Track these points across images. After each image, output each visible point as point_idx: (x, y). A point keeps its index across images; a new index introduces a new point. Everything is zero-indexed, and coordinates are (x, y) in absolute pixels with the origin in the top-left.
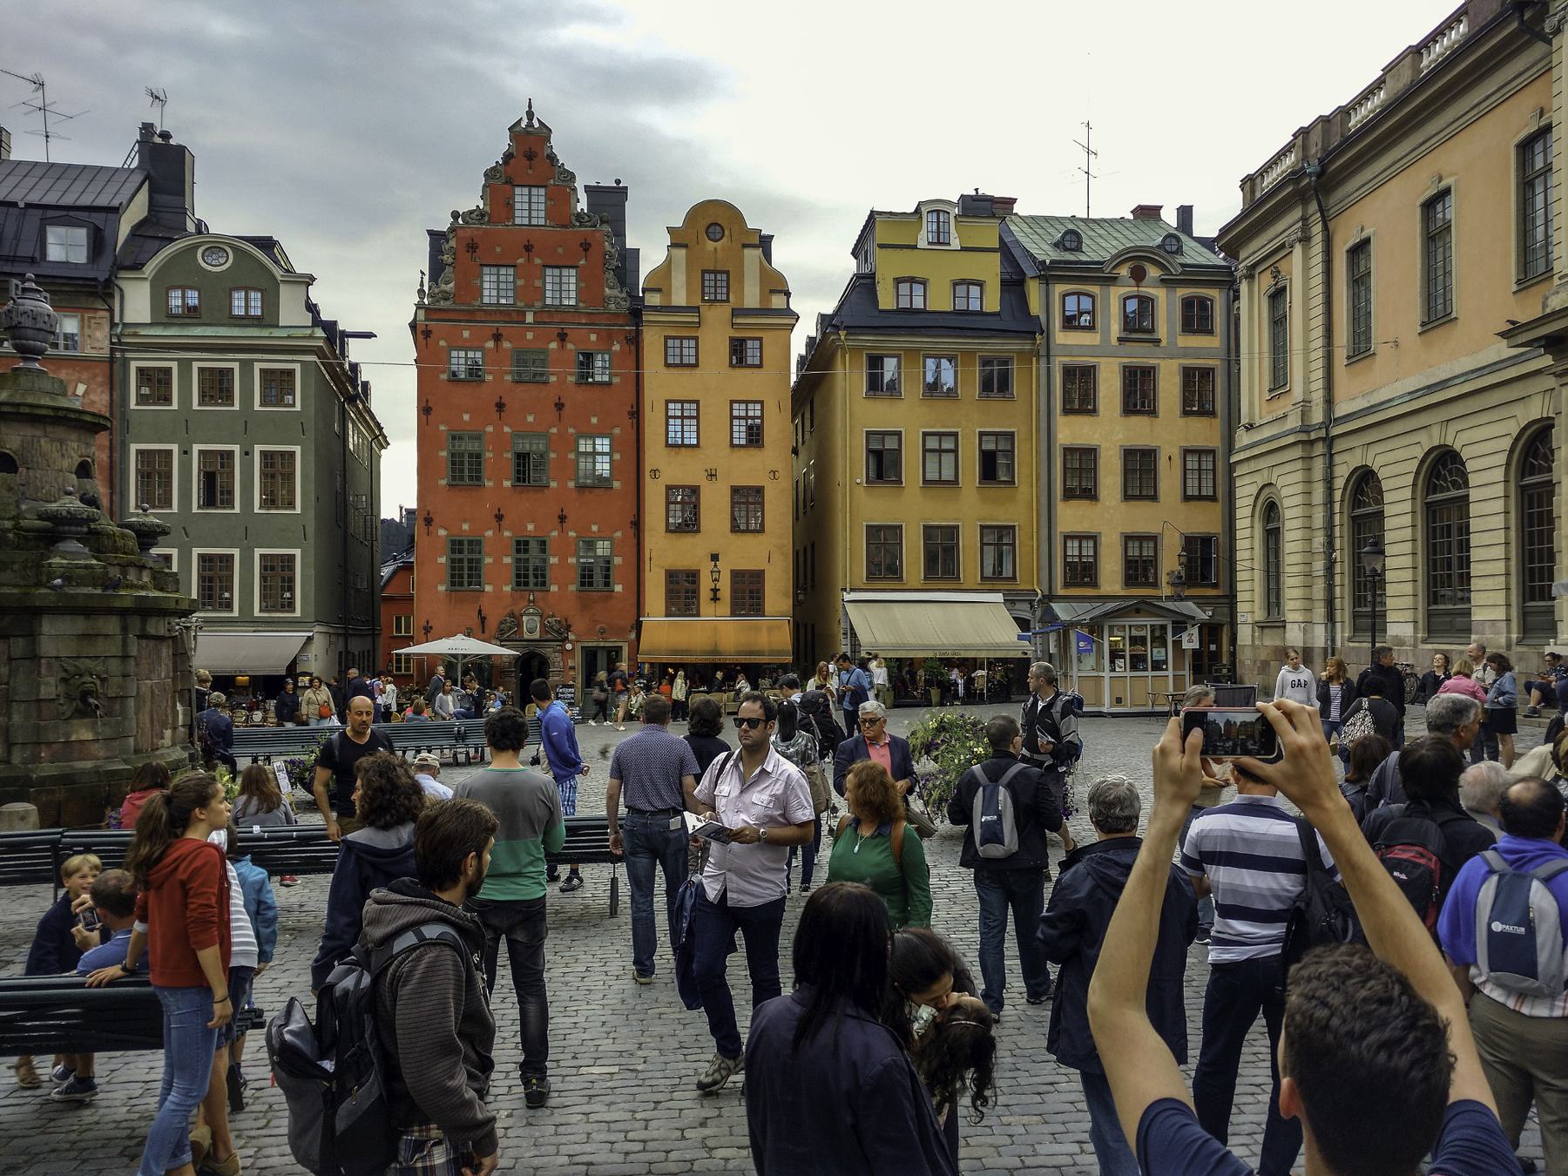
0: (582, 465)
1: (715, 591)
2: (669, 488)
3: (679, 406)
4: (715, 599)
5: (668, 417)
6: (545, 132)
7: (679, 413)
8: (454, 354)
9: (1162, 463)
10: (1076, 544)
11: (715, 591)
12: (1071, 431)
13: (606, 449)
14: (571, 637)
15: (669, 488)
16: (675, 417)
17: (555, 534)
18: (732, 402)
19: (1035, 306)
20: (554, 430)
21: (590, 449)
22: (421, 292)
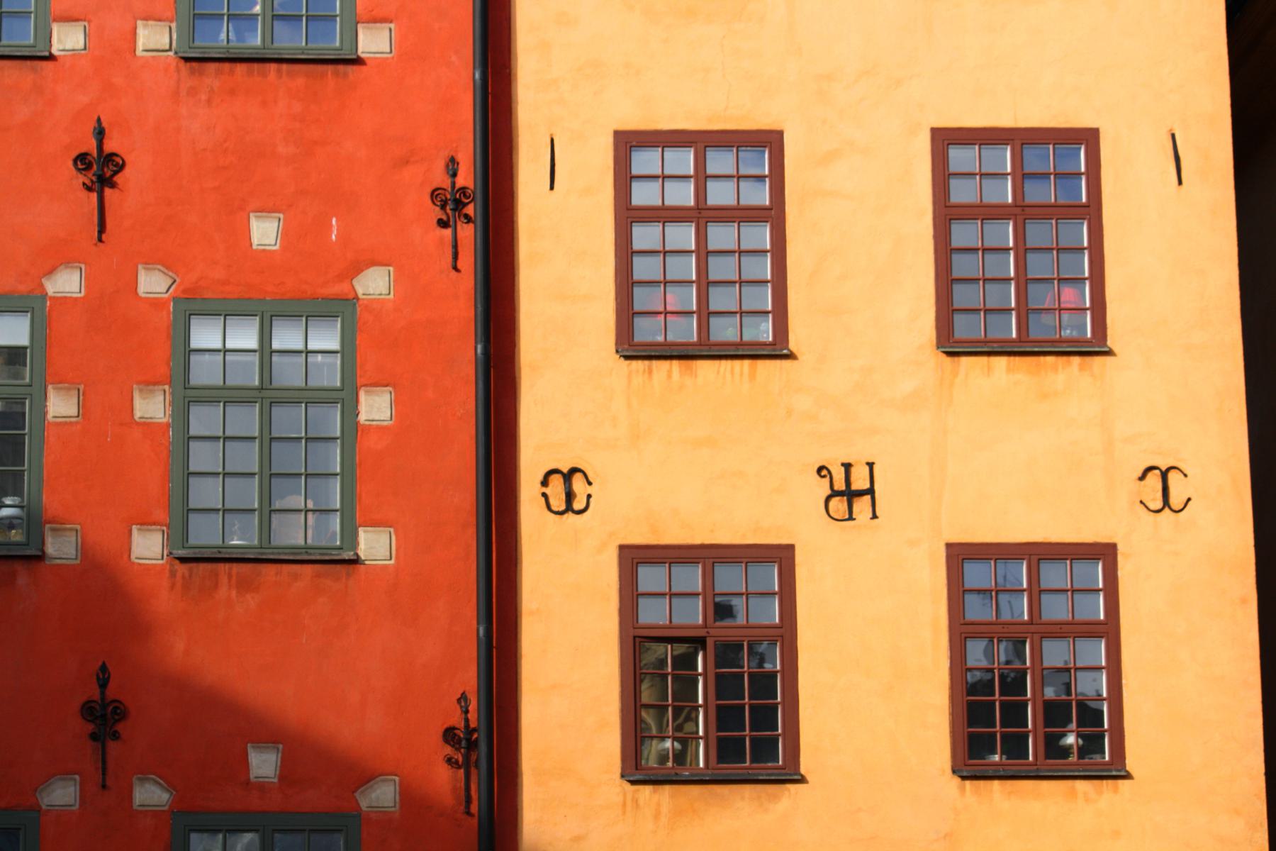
0: (203, 457)
2: (634, 558)
3: (683, 161)
5: (628, 216)
7: (683, 195)
15: (634, 558)
16: (664, 215)
17: (62, 795)
18: (944, 140)
20: (66, 283)
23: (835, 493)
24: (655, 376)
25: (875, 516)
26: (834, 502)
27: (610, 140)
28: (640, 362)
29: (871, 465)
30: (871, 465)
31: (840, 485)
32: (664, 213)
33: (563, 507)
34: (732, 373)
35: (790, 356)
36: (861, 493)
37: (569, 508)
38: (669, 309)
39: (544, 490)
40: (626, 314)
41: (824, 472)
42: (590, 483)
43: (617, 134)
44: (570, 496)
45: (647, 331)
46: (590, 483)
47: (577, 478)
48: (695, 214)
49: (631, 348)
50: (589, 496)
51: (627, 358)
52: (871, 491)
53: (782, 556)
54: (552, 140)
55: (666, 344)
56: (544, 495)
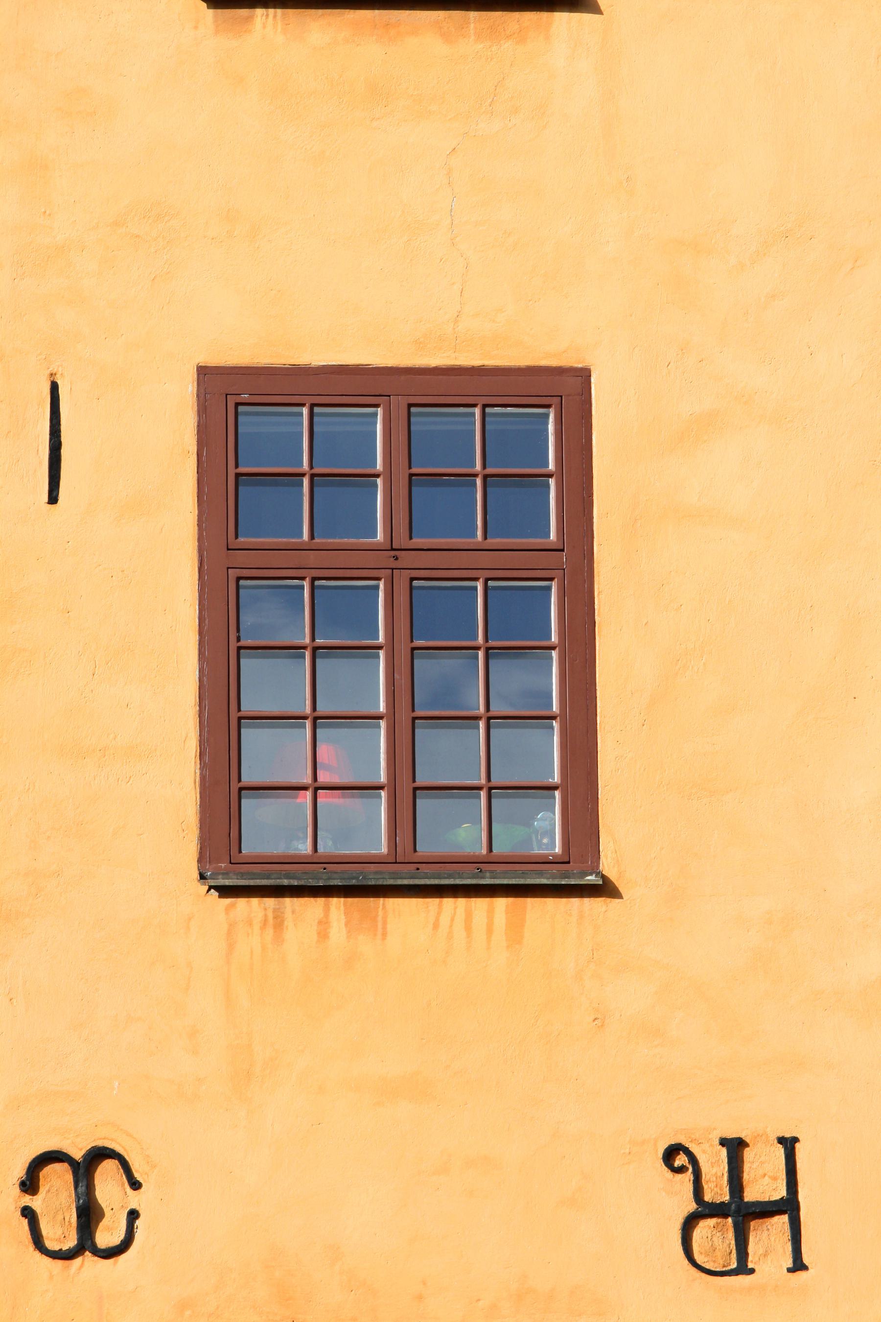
23: (705, 1210)
24: (290, 933)
25: (798, 1265)
26: (704, 1230)
27: (190, 388)
28: (255, 901)
29: (789, 1144)
30: (789, 1144)
31: (717, 1190)
32: (312, 559)
33: (71, 1242)
34: (468, 928)
35: (605, 889)
36: (766, 1210)
37: (86, 1244)
38: (324, 777)
39: (26, 1200)
40: (225, 791)
41: (681, 1160)
42: (135, 1185)
43: (207, 376)
44: (88, 1215)
45: (273, 829)
46: (135, 1185)
47: (107, 1171)
48: (385, 559)
49: (236, 871)
50: (133, 1215)
51: (225, 891)
52: (789, 1206)
54: (54, 388)
55: (315, 860)
56: (28, 1213)
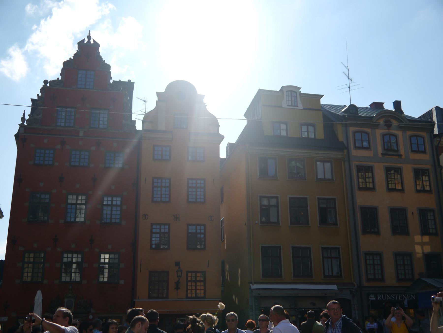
1: (178, 283)
4: (177, 288)
6: (96, 45)
8: (38, 151)
9: (409, 216)
10: (371, 258)
11: (178, 283)
12: (363, 199)
13: (119, 203)
14: (93, 311)
15: (152, 224)
19: (341, 138)
21: (110, 203)
22: (23, 119)
45: (155, 199)
53: (169, 225)
